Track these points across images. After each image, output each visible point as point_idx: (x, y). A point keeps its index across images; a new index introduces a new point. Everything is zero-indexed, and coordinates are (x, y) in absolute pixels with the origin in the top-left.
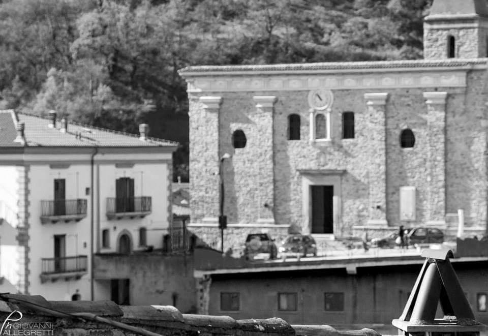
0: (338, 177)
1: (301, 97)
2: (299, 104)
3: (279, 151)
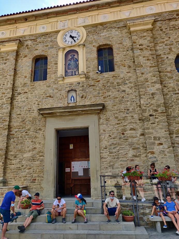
0: (95, 117)
1: (49, 39)
2: (47, 46)
3: (20, 94)
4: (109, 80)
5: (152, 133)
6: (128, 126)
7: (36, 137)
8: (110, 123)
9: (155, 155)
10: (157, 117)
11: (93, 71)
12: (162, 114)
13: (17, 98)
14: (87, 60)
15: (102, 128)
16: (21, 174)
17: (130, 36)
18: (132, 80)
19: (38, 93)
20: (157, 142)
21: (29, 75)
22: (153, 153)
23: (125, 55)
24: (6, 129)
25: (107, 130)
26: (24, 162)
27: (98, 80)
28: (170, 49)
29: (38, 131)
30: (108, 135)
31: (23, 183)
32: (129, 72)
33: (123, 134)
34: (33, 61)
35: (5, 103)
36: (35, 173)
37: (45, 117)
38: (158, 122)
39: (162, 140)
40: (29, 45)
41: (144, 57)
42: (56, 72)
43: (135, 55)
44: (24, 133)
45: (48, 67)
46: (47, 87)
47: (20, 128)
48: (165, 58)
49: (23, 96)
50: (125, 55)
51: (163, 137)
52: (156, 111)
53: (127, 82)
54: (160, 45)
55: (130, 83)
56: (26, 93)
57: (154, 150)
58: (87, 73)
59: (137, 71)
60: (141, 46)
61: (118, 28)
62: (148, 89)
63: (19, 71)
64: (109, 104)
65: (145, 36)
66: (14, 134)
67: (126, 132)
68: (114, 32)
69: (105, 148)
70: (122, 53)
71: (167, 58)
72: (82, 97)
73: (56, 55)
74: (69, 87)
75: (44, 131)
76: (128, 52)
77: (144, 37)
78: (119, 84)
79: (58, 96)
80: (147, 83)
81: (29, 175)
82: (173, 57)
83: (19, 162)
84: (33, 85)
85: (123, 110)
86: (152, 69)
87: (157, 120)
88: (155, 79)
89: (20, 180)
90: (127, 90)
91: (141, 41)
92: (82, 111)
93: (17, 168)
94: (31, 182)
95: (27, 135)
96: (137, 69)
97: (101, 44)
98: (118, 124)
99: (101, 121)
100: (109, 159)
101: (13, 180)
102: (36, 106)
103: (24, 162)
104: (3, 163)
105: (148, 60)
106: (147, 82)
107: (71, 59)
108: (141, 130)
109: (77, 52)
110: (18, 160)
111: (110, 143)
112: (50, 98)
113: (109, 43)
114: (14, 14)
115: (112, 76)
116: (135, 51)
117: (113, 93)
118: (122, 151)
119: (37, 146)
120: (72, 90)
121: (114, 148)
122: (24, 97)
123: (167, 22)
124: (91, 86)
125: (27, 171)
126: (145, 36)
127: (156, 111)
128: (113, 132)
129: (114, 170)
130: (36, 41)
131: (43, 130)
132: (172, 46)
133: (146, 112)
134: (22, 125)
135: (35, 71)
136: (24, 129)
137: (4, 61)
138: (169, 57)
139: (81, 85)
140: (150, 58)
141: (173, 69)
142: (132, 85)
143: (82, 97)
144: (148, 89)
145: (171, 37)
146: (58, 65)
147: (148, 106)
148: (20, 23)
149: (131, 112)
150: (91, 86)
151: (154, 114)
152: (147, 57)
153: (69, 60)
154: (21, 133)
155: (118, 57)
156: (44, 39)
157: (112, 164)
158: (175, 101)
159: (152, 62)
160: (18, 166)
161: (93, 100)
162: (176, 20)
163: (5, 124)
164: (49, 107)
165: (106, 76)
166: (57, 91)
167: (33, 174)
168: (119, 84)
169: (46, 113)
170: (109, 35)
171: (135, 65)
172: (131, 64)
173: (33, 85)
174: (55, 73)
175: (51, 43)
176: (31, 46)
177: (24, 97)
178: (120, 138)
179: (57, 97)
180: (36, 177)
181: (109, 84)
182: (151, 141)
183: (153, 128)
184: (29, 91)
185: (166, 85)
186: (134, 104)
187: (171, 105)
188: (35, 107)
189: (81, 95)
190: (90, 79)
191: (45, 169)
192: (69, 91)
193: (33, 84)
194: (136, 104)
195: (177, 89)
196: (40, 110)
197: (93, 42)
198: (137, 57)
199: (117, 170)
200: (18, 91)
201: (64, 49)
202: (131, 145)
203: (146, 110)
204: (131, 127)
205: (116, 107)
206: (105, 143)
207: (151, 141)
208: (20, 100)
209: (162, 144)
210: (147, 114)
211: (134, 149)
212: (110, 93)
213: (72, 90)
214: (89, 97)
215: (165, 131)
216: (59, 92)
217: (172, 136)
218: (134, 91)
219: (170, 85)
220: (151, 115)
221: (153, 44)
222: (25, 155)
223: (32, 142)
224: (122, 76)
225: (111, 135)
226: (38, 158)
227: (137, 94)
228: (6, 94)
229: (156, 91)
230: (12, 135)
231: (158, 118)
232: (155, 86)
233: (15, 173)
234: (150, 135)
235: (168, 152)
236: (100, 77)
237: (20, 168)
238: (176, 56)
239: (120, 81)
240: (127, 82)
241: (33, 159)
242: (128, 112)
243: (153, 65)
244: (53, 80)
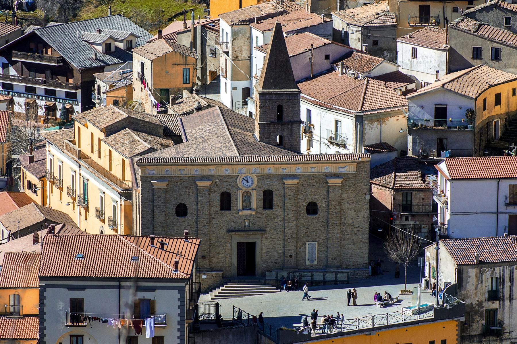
2: (230, 185)
3: (213, 218)
39: (293, 251)
42: (237, 206)
82: (306, 204)
90: (279, 222)
100: (265, 258)
119: (227, 251)
155: (275, 201)
171: (284, 209)
175: (233, 184)
202: (277, 252)
206: (264, 251)
210: (287, 238)
236: (264, 212)
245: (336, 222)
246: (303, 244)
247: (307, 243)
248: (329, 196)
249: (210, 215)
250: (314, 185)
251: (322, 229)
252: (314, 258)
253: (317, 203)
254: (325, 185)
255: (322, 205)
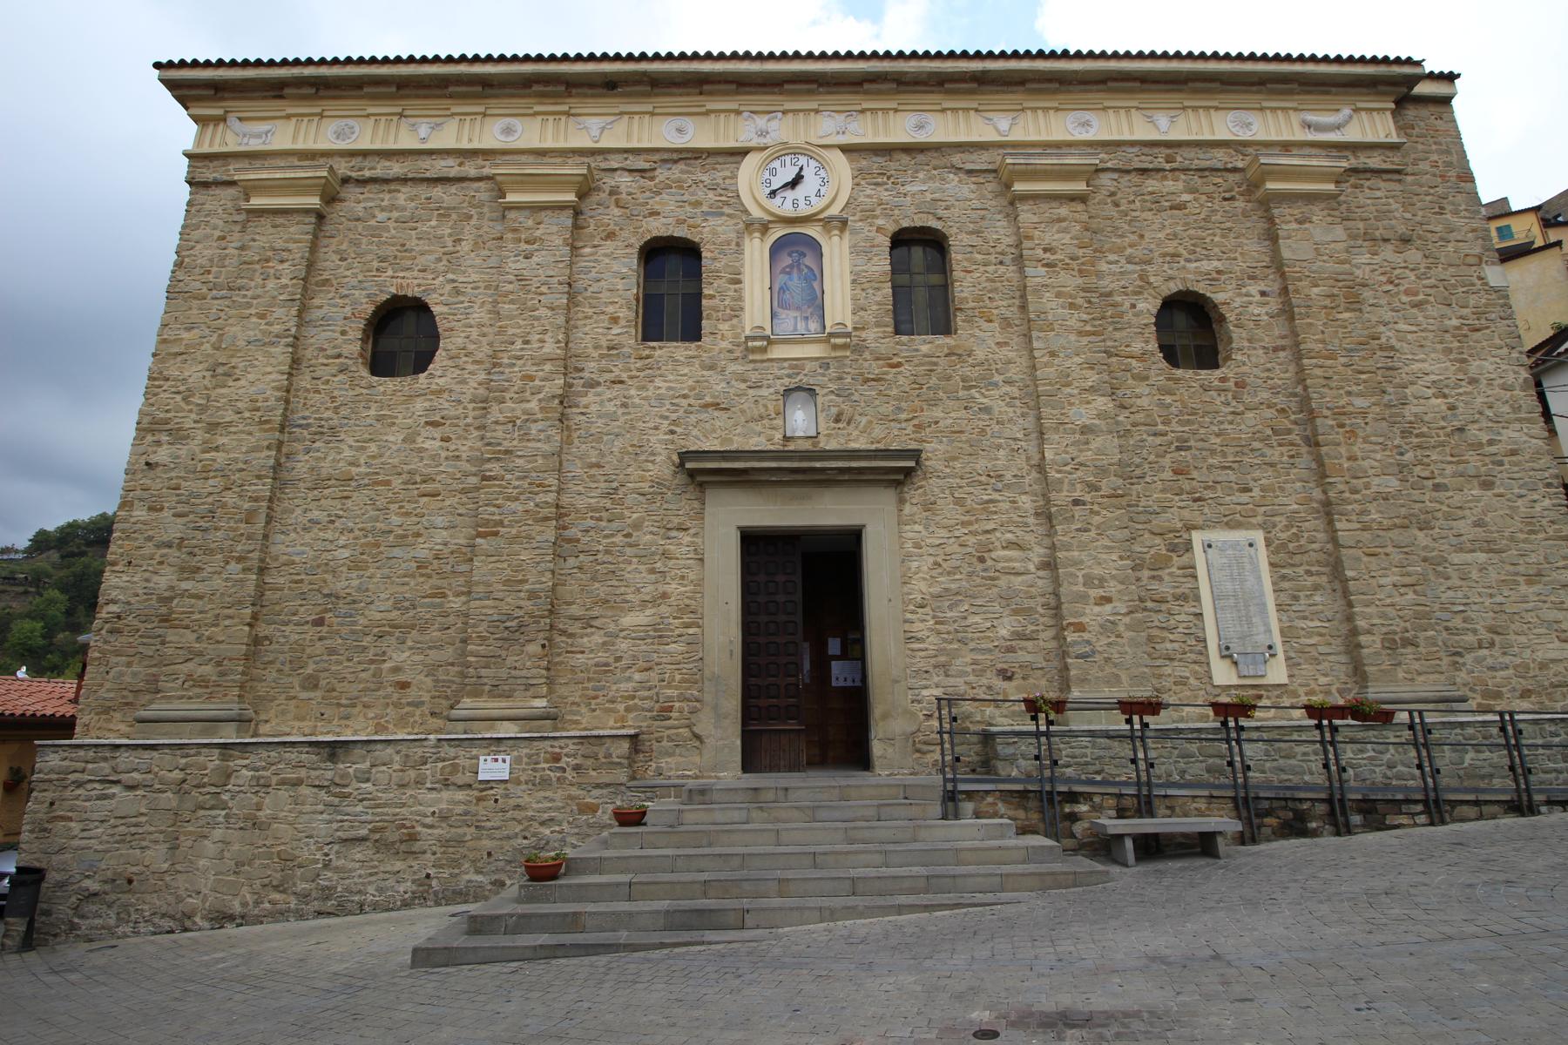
2: (698, 204)
3: (593, 384)
4: (936, 364)
5: (1082, 562)
6: (998, 534)
7: (666, 555)
8: (937, 518)
9: (1086, 636)
10: (1096, 508)
11: (878, 325)
12: (1113, 500)
13: (584, 401)
14: (854, 281)
15: (911, 535)
16: (614, 687)
17: (1009, 210)
18: (1013, 372)
19: (670, 388)
20: (1094, 593)
21: (626, 314)
22: (1080, 628)
23: (993, 281)
24: (547, 519)
25: (929, 541)
26: (623, 645)
27: (896, 360)
28: (1141, 278)
29: (674, 533)
30: (931, 559)
31: (623, 719)
32: (1006, 344)
33: (982, 560)
34: (639, 258)
35: (539, 416)
36: (669, 686)
37: (701, 485)
38: (1098, 527)
39: (1113, 588)
40: (623, 189)
41: (1059, 295)
42: (736, 312)
43: (1030, 282)
44: (619, 539)
45: (706, 292)
46: (704, 367)
47: (599, 519)
48: (1127, 305)
49: (608, 394)
50: (993, 281)
51: (1113, 577)
52: (1093, 488)
53: (998, 378)
54: (1112, 257)
55: (1008, 382)
56: (622, 382)
57: (1085, 620)
58: (855, 329)
59: (1035, 344)
60: (1048, 255)
61: (970, 172)
62: (1072, 412)
63: (588, 294)
64: (935, 452)
65: (1064, 220)
66: (578, 541)
67: (994, 554)
68: (958, 189)
69: (922, 607)
70: (982, 269)
71: (1133, 306)
72: (837, 420)
73: (733, 246)
74: (789, 376)
75: (695, 535)
76: (1002, 269)
77: (1060, 220)
78: (968, 384)
79: (745, 406)
80: (1068, 390)
81: (646, 693)
83: (604, 644)
84: (648, 357)
85: (983, 479)
86: (1085, 340)
87: (1097, 520)
88: (1092, 378)
89: (611, 710)
90: (999, 407)
91: (1051, 236)
92: (841, 470)
93: (596, 665)
94: (654, 719)
95: (630, 545)
96: (1035, 334)
97: (905, 224)
98: (963, 524)
99: (907, 509)
100: (932, 642)
101: (584, 710)
102: (662, 437)
103: (623, 645)
104: (543, 646)
105: (1072, 306)
106: (1068, 385)
107: (791, 266)
108: (1042, 551)
109: (815, 247)
110: (598, 638)
111: (936, 590)
112: (716, 413)
113: (933, 223)
114: (565, 57)
115: (946, 351)
116: (1029, 271)
117: (947, 415)
118: (977, 619)
119: (673, 587)
120: (799, 389)
121: (951, 608)
122: (610, 400)
123: (1135, 178)
124: (868, 380)
125: (637, 677)
126: (1064, 220)
127: (1093, 488)
128: (948, 550)
129: (952, 681)
130: (652, 179)
131: (692, 531)
132: (1148, 268)
133: (1061, 491)
134: (608, 505)
135: (645, 296)
136: (615, 525)
137: (524, 246)
138: (1141, 306)
139: (832, 372)
140: (1079, 301)
141: (1150, 347)
142: (1015, 391)
143: (837, 420)
144: (1072, 412)
145: (1147, 235)
146: (746, 287)
147: (1068, 468)
148: (586, 96)
149: (1008, 486)
150: (868, 380)
151: (1087, 498)
152: (1071, 296)
153: (783, 271)
154: (606, 537)
156: (682, 172)
157: (942, 659)
158: (1152, 458)
159: (1085, 317)
160: (602, 656)
161: (878, 431)
162: (1165, 178)
163: (541, 498)
164: (715, 446)
165: (925, 348)
166: (743, 386)
167: (662, 687)
168: (968, 384)
169: (705, 474)
170: (937, 196)
171: (1027, 324)
172: (1013, 313)
173: (648, 357)
174: (731, 318)
176: (629, 194)
177: (610, 400)
178: (970, 574)
179: (743, 412)
180: (670, 699)
181: (934, 381)
182: (1075, 588)
183: (1082, 547)
184: (631, 377)
185: (1127, 402)
186: (1020, 461)
187: (1138, 472)
188: (660, 441)
189: (834, 410)
190: (867, 355)
191: (707, 673)
192: (788, 392)
193: (647, 352)
194: (1028, 459)
195: (1159, 420)
196: (685, 456)
197: (878, 212)
198: (1036, 291)
199: (960, 681)
200: (586, 374)
201: (765, 228)
202: (1005, 598)
203: (1061, 481)
204: (1009, 536)
205: (958, 465)
206: (920, 588)
207: (1075, 588)
208: (594, 408)
209: (1108, 600)
211: (1016, 612)
212: (937, 413)
213: (799, 389)
214: (864, 420)
215: (1121, 558)
216: (751, 392)
217: (1139, 574)
218: (1019, 411)
219: (1139, 401)
220: (1076, 502)
221: (1088, 251)
222: (628, 620)
223: (652, 571)
224: (980, 354)
225: (939, 560)
226: (677, 632)
227: (1030, 423)
228: (537, 382)
229: (1097, 422)
230: (569, 541)
231: (1098, 513)
232: (1094, 405)
233: (590, 685)
234: (1072, 570)
235: (1129, 627)
237: (606, 665)
238: (1159, 302)
239: (974, 373)
240: (998, 378)
241: (658, 633)
242: (1000, 485)
243: (1088, 328)
244: (725, 345)
245: (1360, 402)
246: (1173, 548)
247: (1197, 538)
248: (1286, 254)
249: (568, 363)
250: (1181, 207)
251: (1274, 454)
252: (1262, 640)
253: (1218, 297)
254: (1240, 204)
255: (1244, 305)
